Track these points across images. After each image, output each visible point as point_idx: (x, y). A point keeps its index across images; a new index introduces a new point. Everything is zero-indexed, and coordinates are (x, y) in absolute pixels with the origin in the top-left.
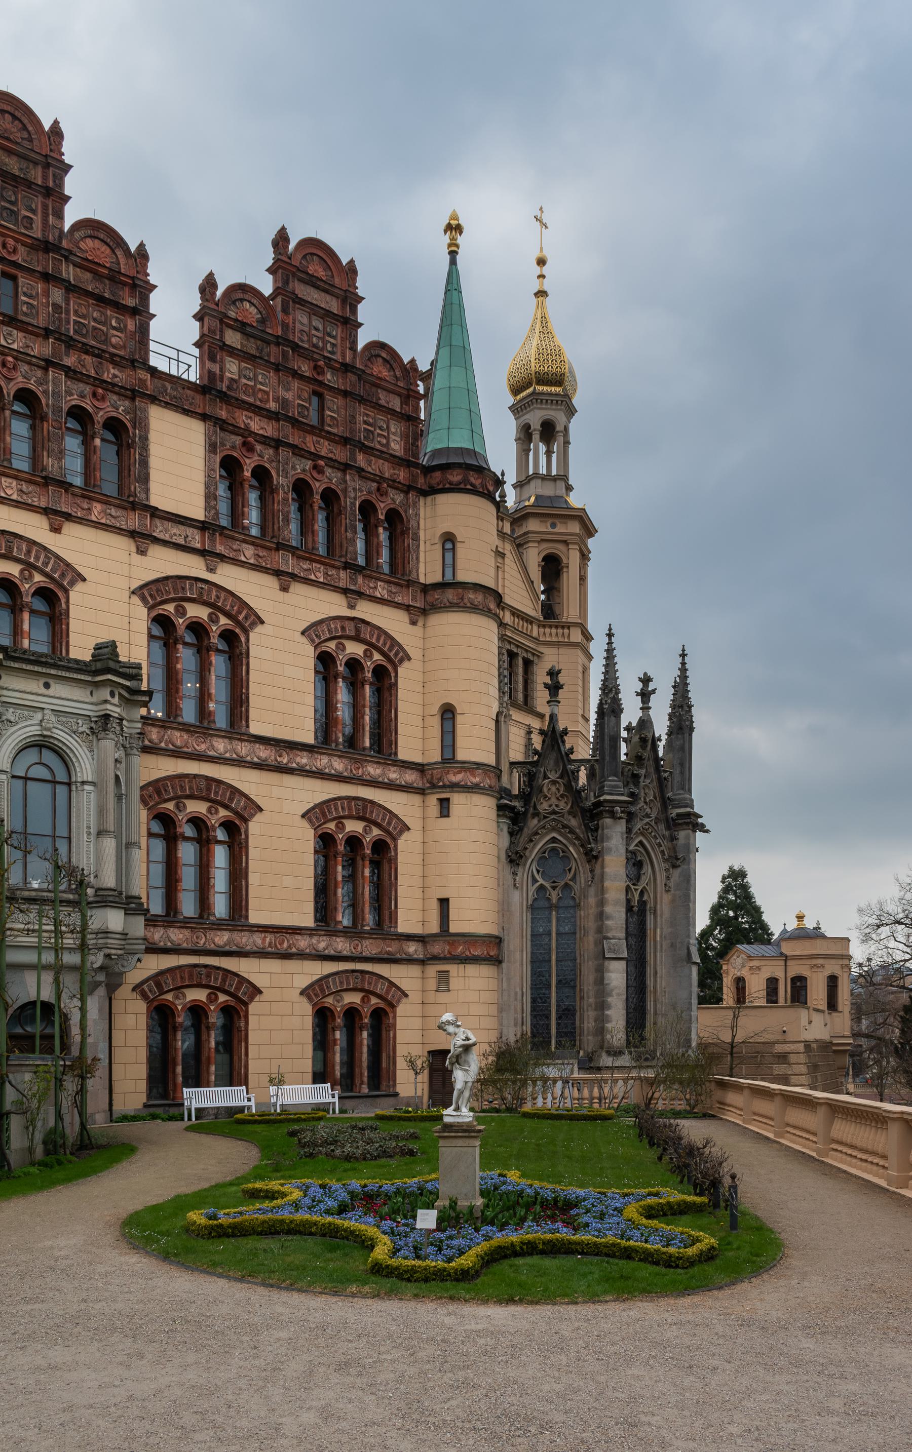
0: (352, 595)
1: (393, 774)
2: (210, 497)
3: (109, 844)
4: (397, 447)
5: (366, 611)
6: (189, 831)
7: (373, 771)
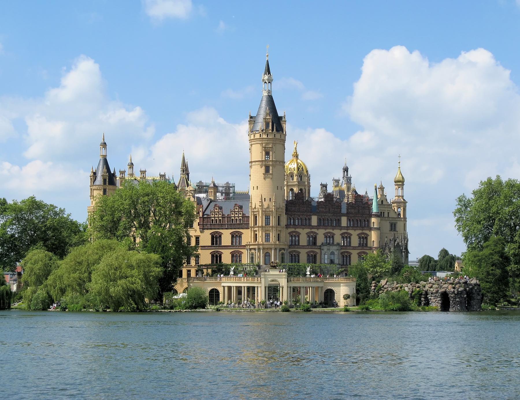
0: (362, 230)
1: (367, 248)
2: (347, 224)
3: (338, 260)
4: (368, 213)
5: (364, 231)
6: (345, 256)
7: (365, 248)
